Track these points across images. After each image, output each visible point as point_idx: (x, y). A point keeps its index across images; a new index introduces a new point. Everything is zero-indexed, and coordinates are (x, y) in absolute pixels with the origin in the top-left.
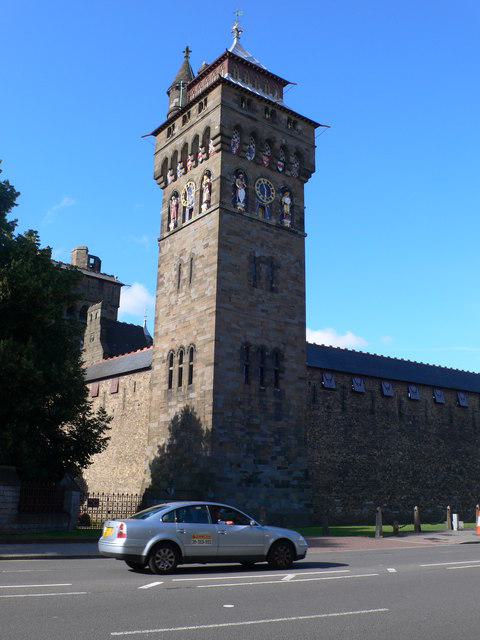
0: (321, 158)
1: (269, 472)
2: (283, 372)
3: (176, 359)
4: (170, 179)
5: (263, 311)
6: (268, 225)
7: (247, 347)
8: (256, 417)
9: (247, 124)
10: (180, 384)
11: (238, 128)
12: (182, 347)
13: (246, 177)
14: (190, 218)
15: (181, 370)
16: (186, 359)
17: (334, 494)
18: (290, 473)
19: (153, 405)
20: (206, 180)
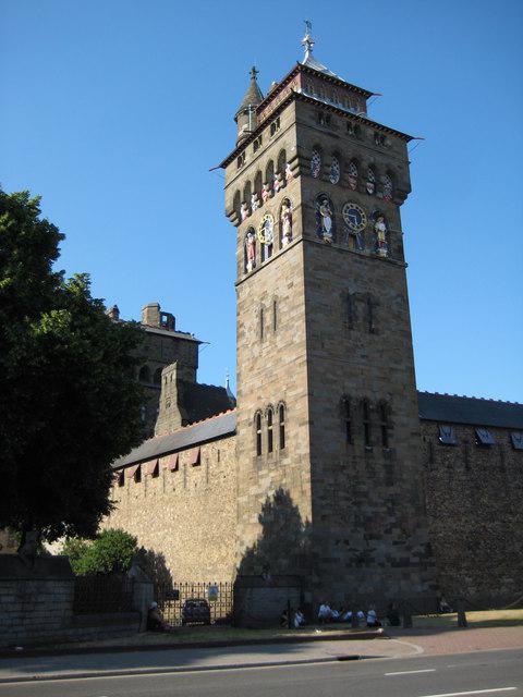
0: (416, 175)
1: (382, 548)
2: (392, 428)
3: (264, 420)
4: (244, 213)
5: (363, 357)
6: (361, 256)
7: (346, 403)
8: (364, 483)
9: (328, 143)
10: (271, 449)
11: (317, 148)
12: (270, 405)
13: (330, 202)
14: (270, 255)
15: (270, 432)
16: (276, 419)
17: (463, 572)
18: (409, 548)
19: (240, 476)
20: (285, 210)
